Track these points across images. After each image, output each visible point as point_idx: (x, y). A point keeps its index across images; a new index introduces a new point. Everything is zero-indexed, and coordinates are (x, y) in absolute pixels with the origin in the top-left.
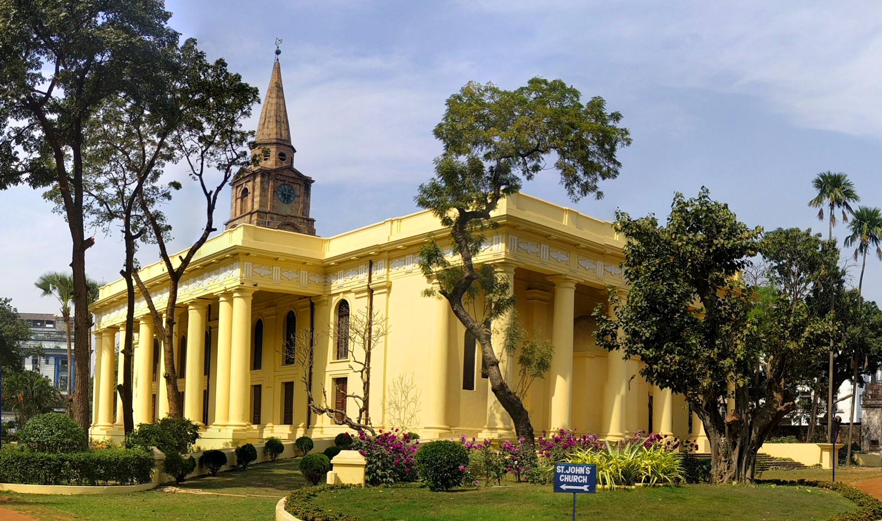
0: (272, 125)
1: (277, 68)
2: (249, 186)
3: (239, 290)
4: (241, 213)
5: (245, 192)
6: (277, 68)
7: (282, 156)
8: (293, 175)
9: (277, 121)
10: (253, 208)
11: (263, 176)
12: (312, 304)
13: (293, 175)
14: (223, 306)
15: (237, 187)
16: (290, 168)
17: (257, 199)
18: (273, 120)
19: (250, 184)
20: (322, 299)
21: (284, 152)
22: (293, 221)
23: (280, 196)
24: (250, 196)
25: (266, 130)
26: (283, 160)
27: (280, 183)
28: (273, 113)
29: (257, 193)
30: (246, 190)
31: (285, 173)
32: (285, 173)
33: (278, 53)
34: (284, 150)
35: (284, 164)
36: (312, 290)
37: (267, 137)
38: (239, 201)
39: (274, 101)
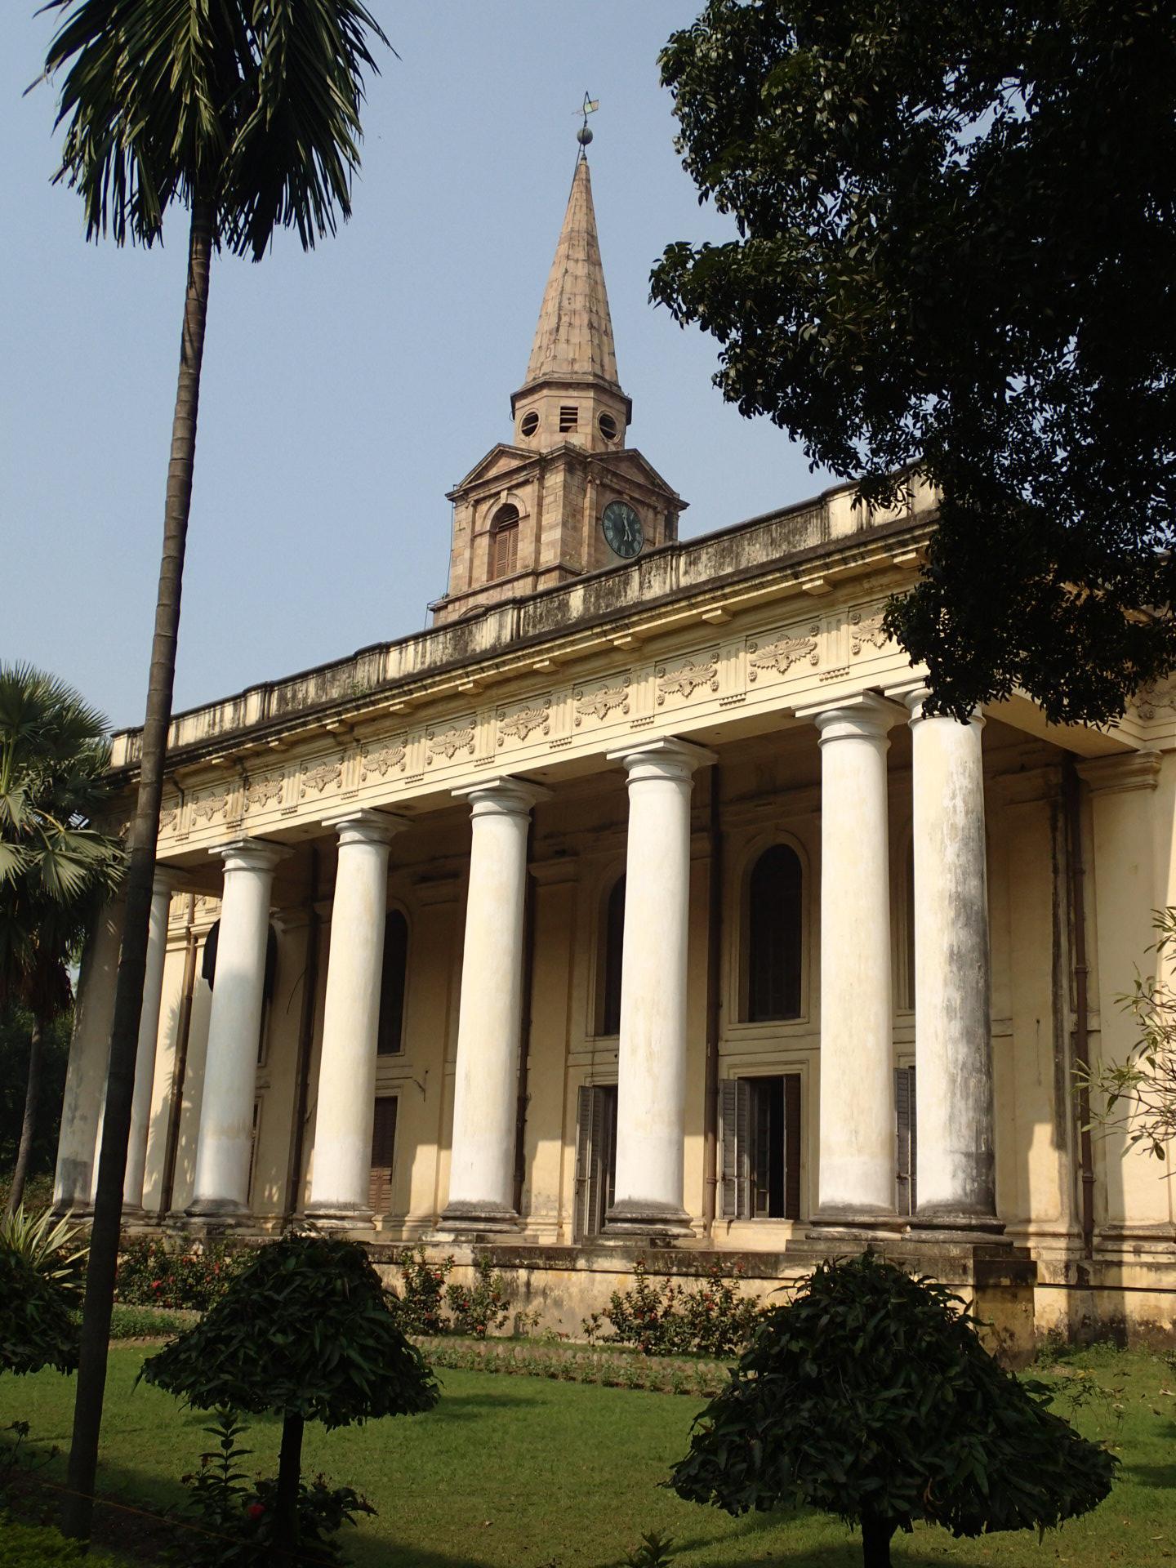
0: (580, 335)
1: (583, 179)
2: (524, 500)
4: (491, 577)
5: (507, 518)
6: (583, 179)
8: (641, 480)
9: (591, 326)
10: (537, 560)
11: (570, 470)
13: (641, 480)
15: (478, 502)
17: (553, 535)
19: (528, 492)
20: (1137, 763)
21: (612, 414)
23: (610, 534)
24: (526, 529)
25: (562, 346)
26: (610, 436)
27: (610, 497)
28: (579, 303)
29: (553, 515)
30: (509, 511)
32: (625, 470)
33: (585, 139)
34: (615, 411)
37: (566, 368)
38: (484, 542)
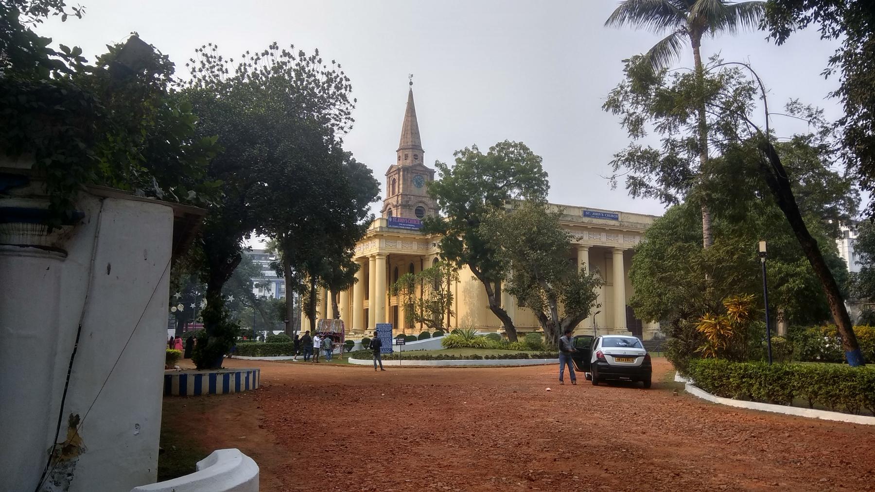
0: (409, 136)
3: (379, 255)
4: (393, 193)
7: (416, 157)
11: (404, 171)
12: (422, 259)
14: (371, 263)
16: (421, 165)
17: (401, 186)
18: (409, 132)
22: (424, 199)
29: (401, 182)
31: (418, 168)
33: (411, 83)
34: (417, 152)
35: (417, 162)
36: (420, 253)
39: (410, 119)
